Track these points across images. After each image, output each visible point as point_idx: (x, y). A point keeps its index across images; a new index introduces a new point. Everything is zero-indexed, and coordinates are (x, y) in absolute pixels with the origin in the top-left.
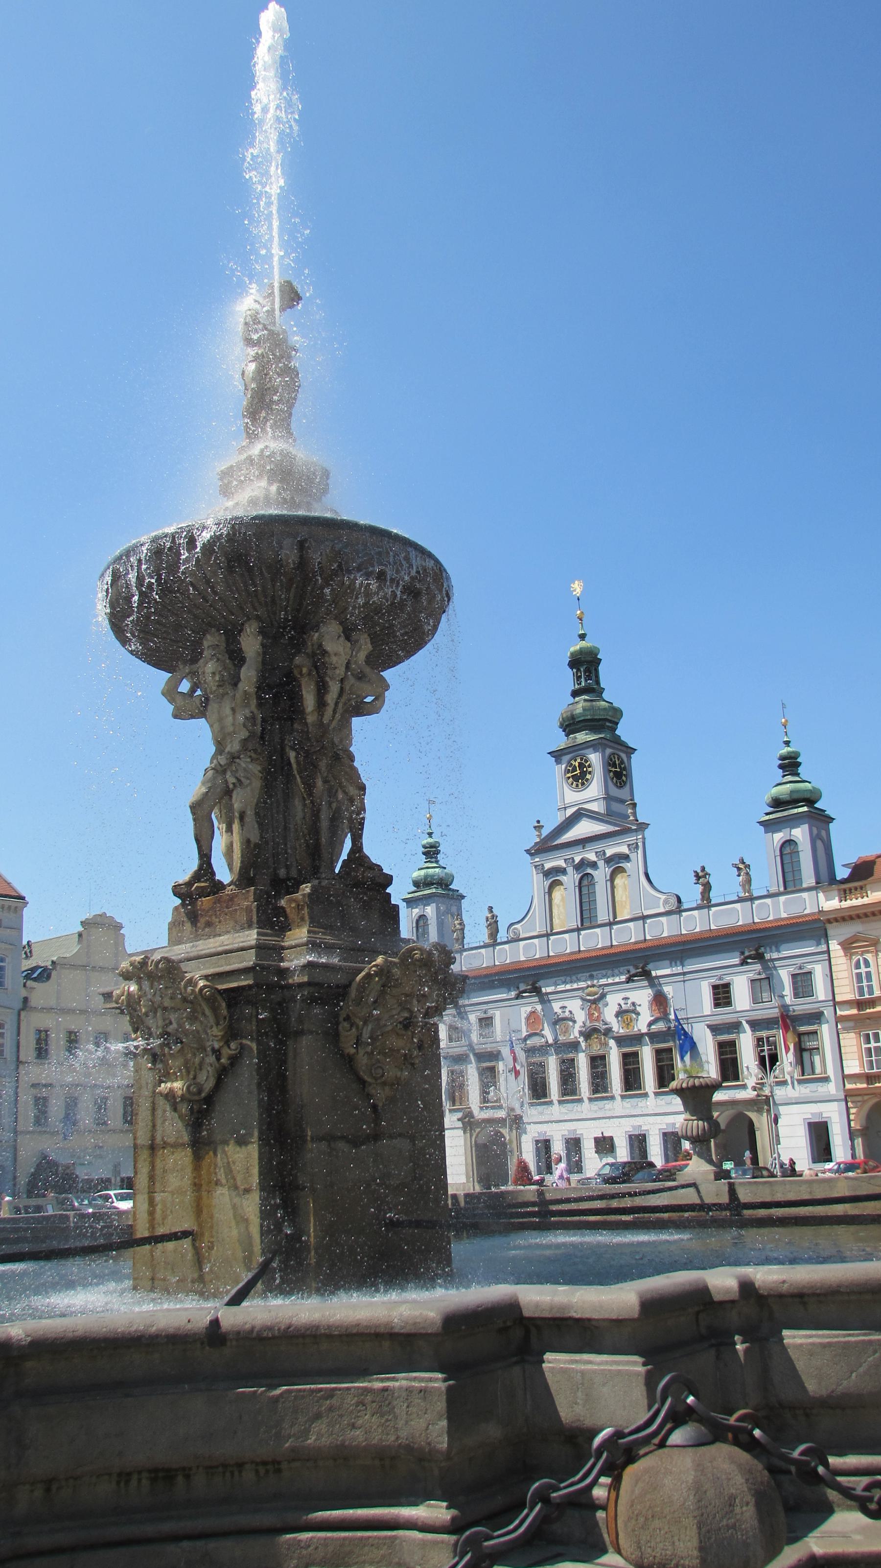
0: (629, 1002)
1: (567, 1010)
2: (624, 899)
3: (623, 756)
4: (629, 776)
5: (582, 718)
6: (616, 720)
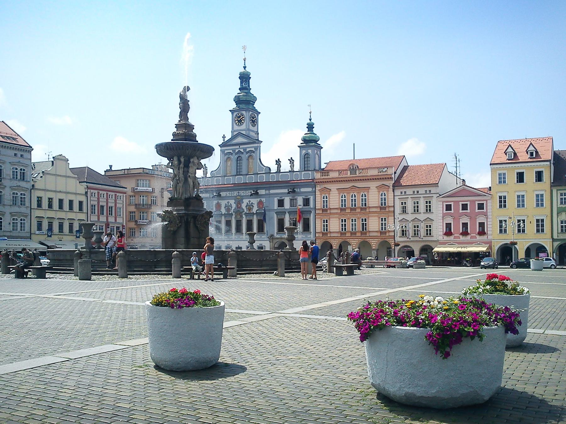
0: (251, 202)
1: (230, 203)
3: (256, 115)
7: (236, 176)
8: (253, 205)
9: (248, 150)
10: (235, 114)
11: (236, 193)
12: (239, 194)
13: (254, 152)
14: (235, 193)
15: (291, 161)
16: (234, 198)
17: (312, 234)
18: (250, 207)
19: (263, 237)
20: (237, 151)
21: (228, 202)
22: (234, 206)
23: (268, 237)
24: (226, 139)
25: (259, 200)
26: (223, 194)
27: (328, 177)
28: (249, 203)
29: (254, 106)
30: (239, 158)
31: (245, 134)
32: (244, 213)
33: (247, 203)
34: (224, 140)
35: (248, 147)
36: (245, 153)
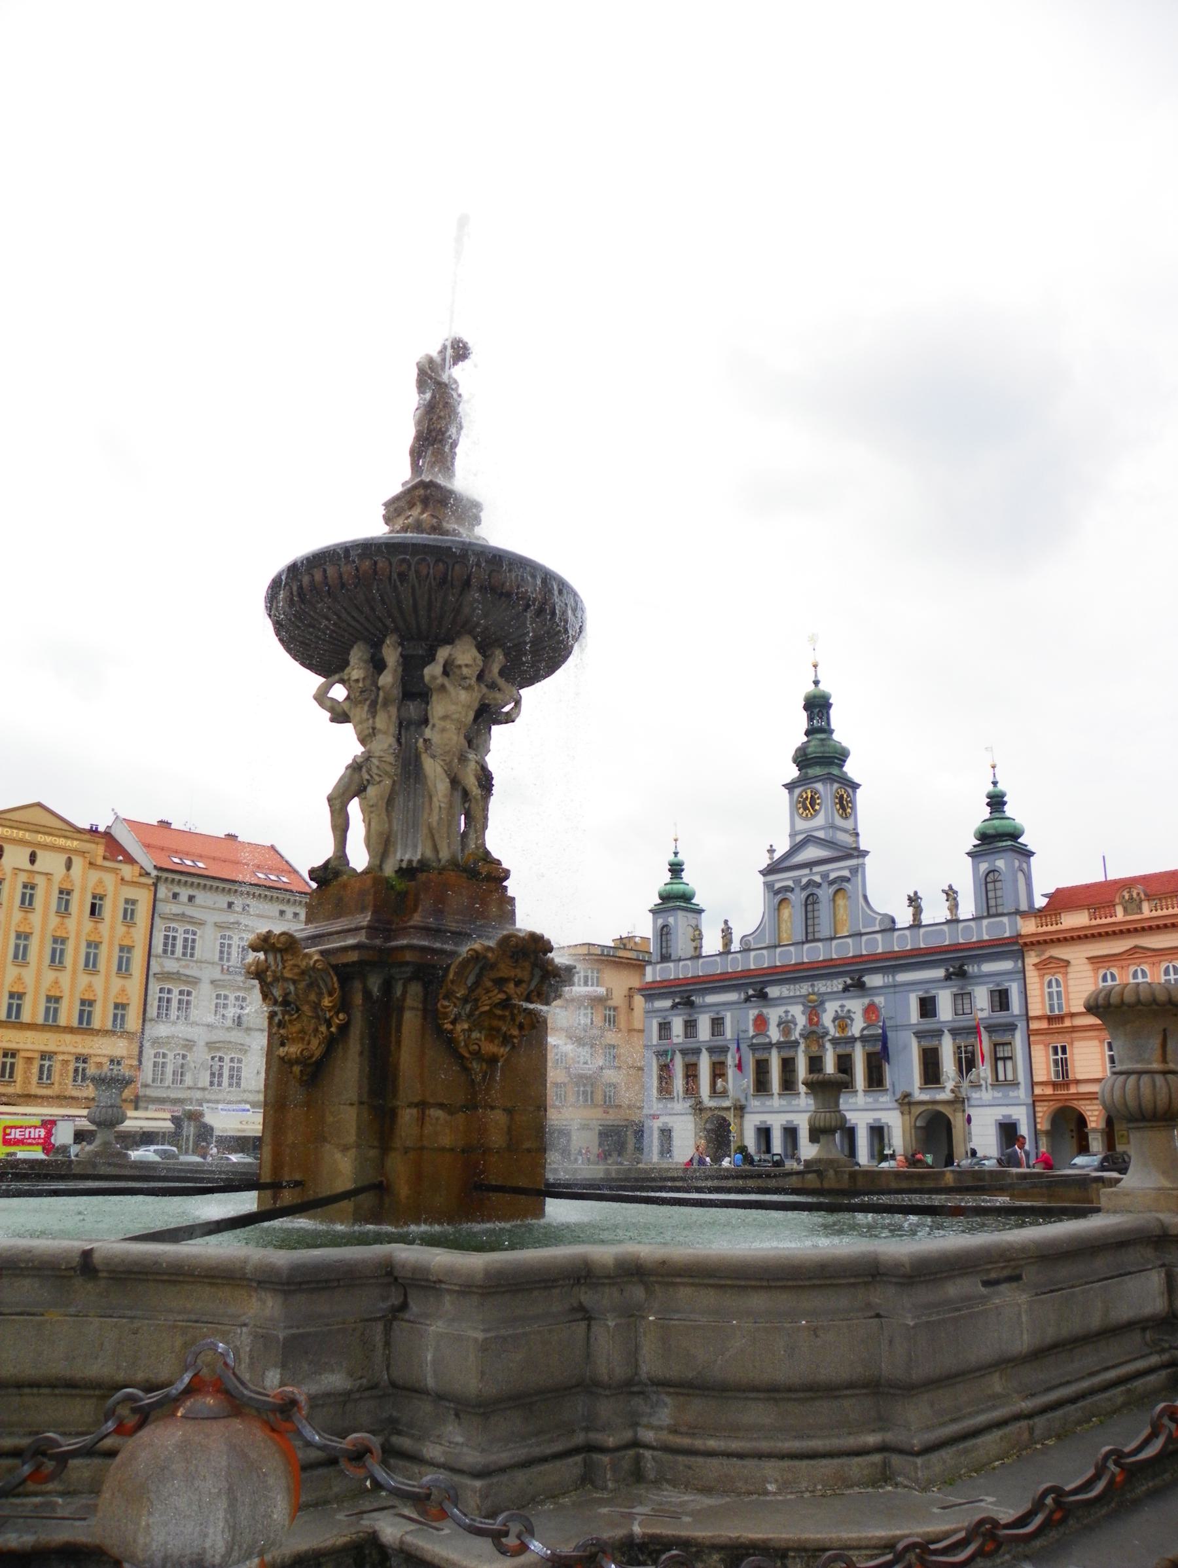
0: (846, 1009)
1: (790, 1014)
2: (845, 917)
4: (853, 808)
7: (803, 943)
8: (852, 1015)
9: (833, 876)
10: (797, 791)
13: (848, 880)
14: (804, 988)
15: (951, 894)
16: (801, 1000)
17: (1022, 1086)
18: (842, 1020)
19: (881, 1099)
20: (804, 881)
21: (787, 1012)
22: (802, 1021)
23: (896, 1101)
24: (777, 856)
25: (866, 1001)
26: (773, 992)
27: (1059, 927)
28: (842, 1011)
29: (845, 769)
30: (811, 898)
32: (830, 1037)
34: (771, 858)
35: (833, 870)
36: (825, 885)
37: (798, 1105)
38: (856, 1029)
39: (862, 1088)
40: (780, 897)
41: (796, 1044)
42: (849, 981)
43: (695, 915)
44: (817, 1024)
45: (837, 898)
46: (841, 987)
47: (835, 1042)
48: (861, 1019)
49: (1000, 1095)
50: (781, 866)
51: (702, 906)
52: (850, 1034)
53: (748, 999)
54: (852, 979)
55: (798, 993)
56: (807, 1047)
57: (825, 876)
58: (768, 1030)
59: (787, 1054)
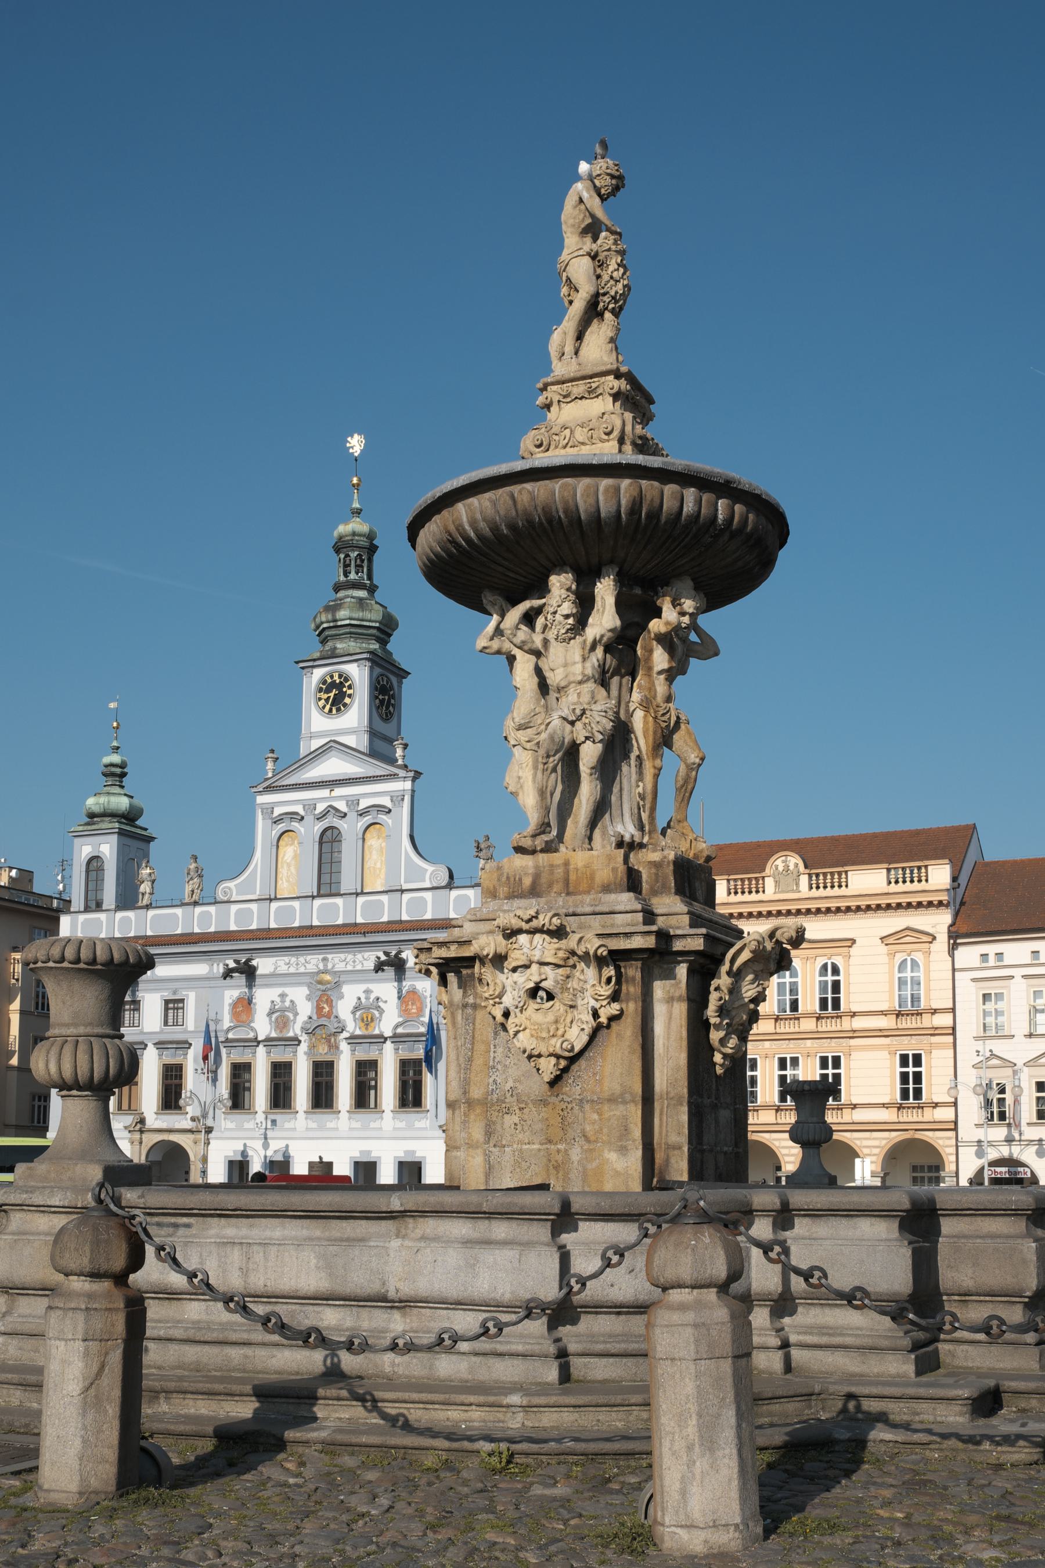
0: (373, 996)
1: (288, 999)
2: (378, 865)
3: (394, 680)
4: (397, 706)
5: (347, 622)
6: (389, 631)
8: (381, 1004)
9: (364, 804)
11: (314, 962)
12: (325, 966)
14: (312, 962)
16: (307, 979)
18: (367, 1012)
19: (418, 1124)
20: (321, 807)
21: (283, 996)
22: (305, 1010)
23: (440, 1127)
26: (264, 965)
28: (367, 998)
29: (389, 647)
30: (329, 833)
31: (354, 746)
32: (345, 1035)
33: (359, 999)
35: (365, 795)
36: (352, 816)
37: (337, 1129)
38: (386, 1026)
39: (263, 1108)
40: (281, 827)
41: (296, 1041)
42: (383, 958)
43: (141, 845)
44: (328, 1016)
45: (368, 835)
46: (370, 965)
47: (353, 1039)
48: (396, 1012)
49: (403, 1125)
50: (284, 783)
51: (152, 832)
52: (377, 1032)
53: (228, 974)
54: (386, 954)
55: (302, 970)
56: (312, 1047)
57: (353, 802)
58: (252, 1021)
59: (281, 1055)
